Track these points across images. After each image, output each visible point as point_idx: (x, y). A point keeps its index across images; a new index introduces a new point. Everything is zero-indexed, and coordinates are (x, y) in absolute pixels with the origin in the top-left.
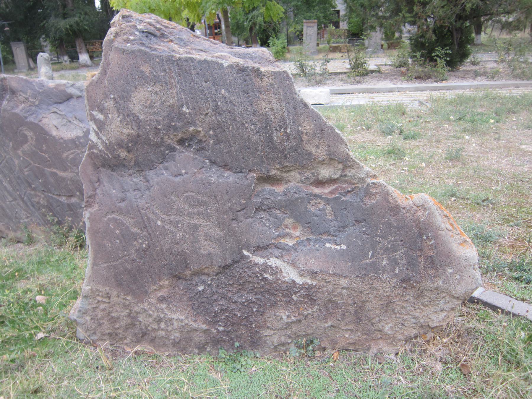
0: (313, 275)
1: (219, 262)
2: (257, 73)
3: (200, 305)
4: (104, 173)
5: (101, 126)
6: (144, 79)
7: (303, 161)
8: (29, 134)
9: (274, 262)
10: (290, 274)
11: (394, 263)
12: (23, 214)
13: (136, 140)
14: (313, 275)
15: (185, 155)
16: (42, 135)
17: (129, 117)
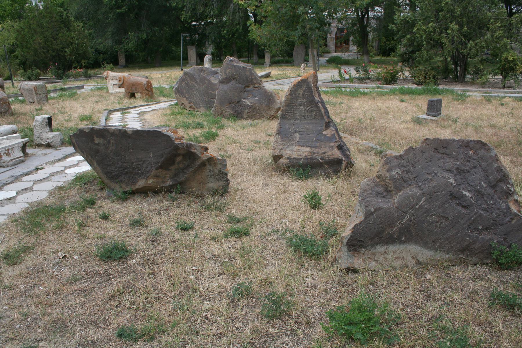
0: (252, 103)
1: (237, 101)
2: (246, 68)
3: (233, 109)
4: (221, 84)
5: (221, 76)
6: (229, 68)
7: (253, 84)
8: (206, 82)
9: (246, 101)
10: (248, 103)
11: (265, 102)
12: (201, 103)
13: (226, 78)
14: (252, 103)
15: (233, 81)
16: (209, 81)
17: (226, 74)
